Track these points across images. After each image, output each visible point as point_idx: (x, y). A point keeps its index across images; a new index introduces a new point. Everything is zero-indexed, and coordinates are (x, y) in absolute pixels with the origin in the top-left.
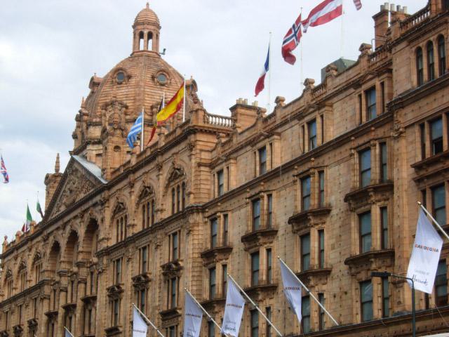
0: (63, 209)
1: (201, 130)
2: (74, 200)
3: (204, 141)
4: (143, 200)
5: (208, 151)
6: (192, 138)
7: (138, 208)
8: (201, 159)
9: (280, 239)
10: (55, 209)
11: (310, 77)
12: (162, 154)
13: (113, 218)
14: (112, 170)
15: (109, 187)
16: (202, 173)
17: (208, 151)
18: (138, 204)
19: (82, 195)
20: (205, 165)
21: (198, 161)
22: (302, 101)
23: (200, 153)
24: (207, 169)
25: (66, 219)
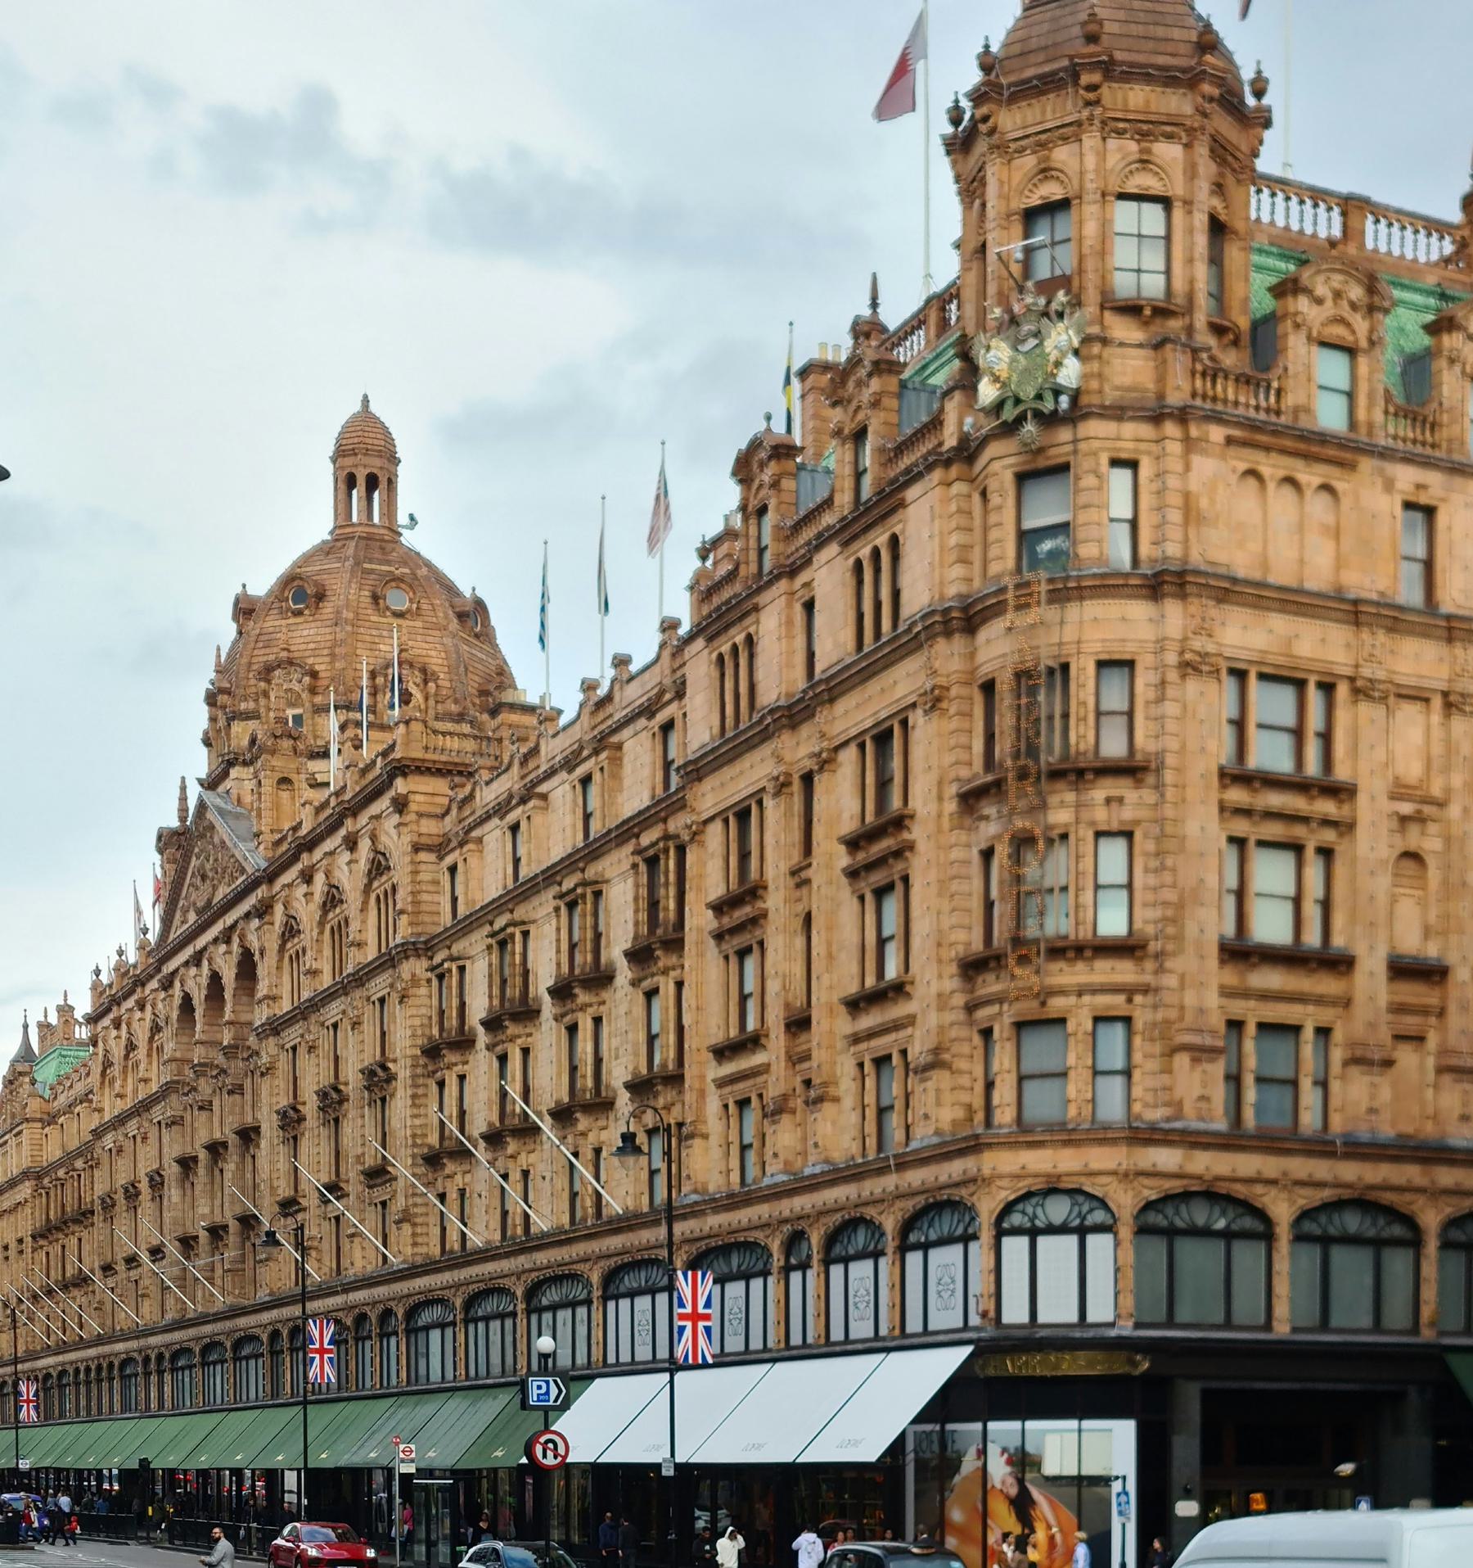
0: (192, 917)
1: (418, 768)
2: (209, 901)
3: (422, 790)
4: (331, 915)
5: (436, 816)
6: (400, 785)
7: (321, 932)
8: (420, 835)
9: (544, 1028)
10: (178, 915)
11: (593, 674)
12: (355, 815)
13: (282, 949)
14: (278, 836)
15: (270, 876)
16: (423, 867)
17: (436, 816)
18: (321, 924)
19: (223, 892)
20: (429, 848)
21: (416, 839)
22: (577, 726)
23: (417, 822)
24: (432, 857)
25: (201, 942)
